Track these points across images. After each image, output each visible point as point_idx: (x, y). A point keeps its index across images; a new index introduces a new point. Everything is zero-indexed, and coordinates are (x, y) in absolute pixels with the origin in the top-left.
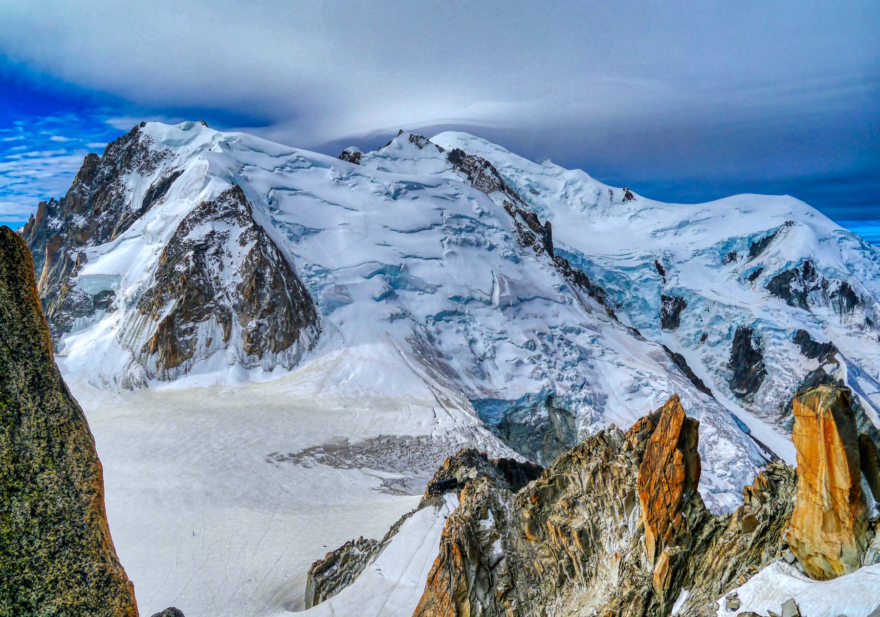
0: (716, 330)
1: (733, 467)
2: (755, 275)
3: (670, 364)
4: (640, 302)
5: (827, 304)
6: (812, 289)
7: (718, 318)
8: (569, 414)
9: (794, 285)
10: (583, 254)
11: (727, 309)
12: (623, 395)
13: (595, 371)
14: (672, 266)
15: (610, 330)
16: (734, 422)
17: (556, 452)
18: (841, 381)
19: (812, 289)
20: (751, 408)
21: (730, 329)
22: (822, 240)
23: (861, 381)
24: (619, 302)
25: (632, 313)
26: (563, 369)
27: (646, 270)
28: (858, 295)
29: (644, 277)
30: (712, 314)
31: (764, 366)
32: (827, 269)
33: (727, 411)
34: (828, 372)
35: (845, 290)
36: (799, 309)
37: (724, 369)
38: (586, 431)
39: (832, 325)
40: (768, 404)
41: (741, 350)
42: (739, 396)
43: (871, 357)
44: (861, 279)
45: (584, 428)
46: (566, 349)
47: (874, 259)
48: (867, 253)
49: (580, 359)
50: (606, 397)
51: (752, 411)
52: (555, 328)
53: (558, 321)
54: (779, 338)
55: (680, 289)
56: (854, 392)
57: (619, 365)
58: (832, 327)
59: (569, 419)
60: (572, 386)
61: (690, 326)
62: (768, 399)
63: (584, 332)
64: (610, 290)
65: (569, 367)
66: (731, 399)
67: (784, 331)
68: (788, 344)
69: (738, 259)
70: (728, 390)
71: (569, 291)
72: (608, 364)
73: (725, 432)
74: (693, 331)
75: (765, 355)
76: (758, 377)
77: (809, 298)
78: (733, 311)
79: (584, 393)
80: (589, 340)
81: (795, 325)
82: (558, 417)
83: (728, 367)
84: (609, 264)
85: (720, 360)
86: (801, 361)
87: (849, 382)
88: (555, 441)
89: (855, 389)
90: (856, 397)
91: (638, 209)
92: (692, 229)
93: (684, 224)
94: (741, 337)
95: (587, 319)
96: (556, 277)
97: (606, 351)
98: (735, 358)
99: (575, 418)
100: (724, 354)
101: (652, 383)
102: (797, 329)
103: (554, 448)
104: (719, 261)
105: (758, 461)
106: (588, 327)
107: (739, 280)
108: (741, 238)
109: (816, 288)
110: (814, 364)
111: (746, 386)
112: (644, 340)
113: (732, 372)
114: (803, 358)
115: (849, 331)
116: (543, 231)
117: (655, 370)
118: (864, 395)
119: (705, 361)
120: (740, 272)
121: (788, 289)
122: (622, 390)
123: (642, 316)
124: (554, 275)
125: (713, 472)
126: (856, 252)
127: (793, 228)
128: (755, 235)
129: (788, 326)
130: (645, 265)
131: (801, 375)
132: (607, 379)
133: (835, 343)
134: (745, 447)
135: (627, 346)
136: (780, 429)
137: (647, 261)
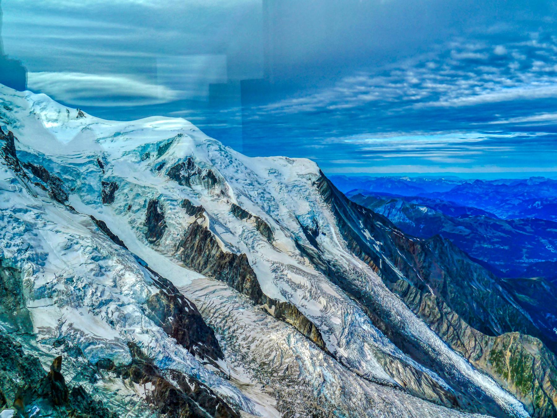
0: (137, 202)
1: (135, 288)
2: (161, 166)
3: (95, 228)
4: (87, 187)
5: (201, 183)
6: (193, 175)
7: (138, 195)
8: (15, 270)
9: (182, 173)
10: (44, 155)
11: (143, 189)
12: (60, 252)
13: (39, 237)
14: (109, 162)
15: (52, 208)
16: (135, 261)
17: (5, 298)
18: (206, 228)
19: (193, 175)
20: (158, 249)
21: (145, 201)
22: (198, 145)
23: (217, 227)
24: (73, 187)
25: (82, 194)
26: (11, 239)
27: (91, 165)
28: (217, 177)
29: (90, 170)
30: (134, 193)
31: (165, 222)
32: (200, 162)
33: (132, 254)
34: (199, 223)
35: (210, 175)
36: (185, 187)
37: (142, 226)
38: (29, 280)
39: (205, 197)
40: (167, 245)
41: (152, 214)
42: (151, 242)
43: (223, 212)
44: (219, 168)
45: (27, 278)
46: (15, 225)
47: (226, 157)
48: (223, 153)
49: (26, 230)
50: (47, 254)
51: (158, 251)
52: (6, 210)
53: (9, 205)
54: (174, 205)
55: (114, 177)
56: (212, 234)
57: (57, 232)
58: (203, 196)
59: (16, 274)
60: (18, 250)
61: (121, 201)
62: (167, 242)
63: (30, 211)
64: (65, 179)
65: (17, 237)
66: (147, 245)
67: (176, 200)
68: (178, 208)
69: (151, 157)
70: (144, 239)
71: (19, 183)
72: (49, 232)
73: (129, 267)
74: (123, 204)
75: (166, 216)
76: (162, 229)
77: (191, 180)
78: (147, 190)
79: (27, 254)
80: (34, 216)
81: (184, 197)
82: (7, 273)
83: (144, 225)
84: (64, 162)
85: (139, 221)
86: (186, 218)
87: (210, 228)
88: (4, 291)
89: (214, 232)
90: (214, 236)
91: (88, 124)
92: (123, 138)
93: (117, 134)
94: (151, 206)
95: (33, 202)
96: (9, 173)
97: (47, 223)
98: (148, 219)
99: (20, 272)
100: (142, 217)
101: (81, 241)
102: (184, 199)
103: (4, 296)
104: (139, 159)
105: (150, 282)
106: (34, 207)
107: (151, 170)
108: (152, 144)
109: (195, 174)
110: (192, 219)
111: (155, 236)
112: (77, 213)
113: (147, 228)
114: (187, 216)
115: (212, 198)
116: (7, 139)
117: (84, 233)
118: (218, 234)
119: (130, 223)
120: (152, 165)
121: (179, 175)
122: (59, 248)
123: (89, 196)
124: (6, 171)
125: (121, 293)
126: (217, 153)
127: (183, 139)
128: (161, 142)
129: (179, 197)
130: (90, 162)
131: (186, 225)
132: (49, 243)
133: (204, 206)
134: (142, 275)
135: (64, 218)
136: (174, 260)
137: (92, 159)
